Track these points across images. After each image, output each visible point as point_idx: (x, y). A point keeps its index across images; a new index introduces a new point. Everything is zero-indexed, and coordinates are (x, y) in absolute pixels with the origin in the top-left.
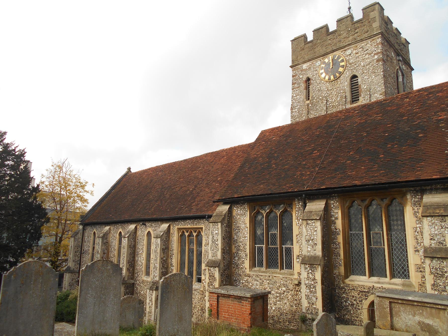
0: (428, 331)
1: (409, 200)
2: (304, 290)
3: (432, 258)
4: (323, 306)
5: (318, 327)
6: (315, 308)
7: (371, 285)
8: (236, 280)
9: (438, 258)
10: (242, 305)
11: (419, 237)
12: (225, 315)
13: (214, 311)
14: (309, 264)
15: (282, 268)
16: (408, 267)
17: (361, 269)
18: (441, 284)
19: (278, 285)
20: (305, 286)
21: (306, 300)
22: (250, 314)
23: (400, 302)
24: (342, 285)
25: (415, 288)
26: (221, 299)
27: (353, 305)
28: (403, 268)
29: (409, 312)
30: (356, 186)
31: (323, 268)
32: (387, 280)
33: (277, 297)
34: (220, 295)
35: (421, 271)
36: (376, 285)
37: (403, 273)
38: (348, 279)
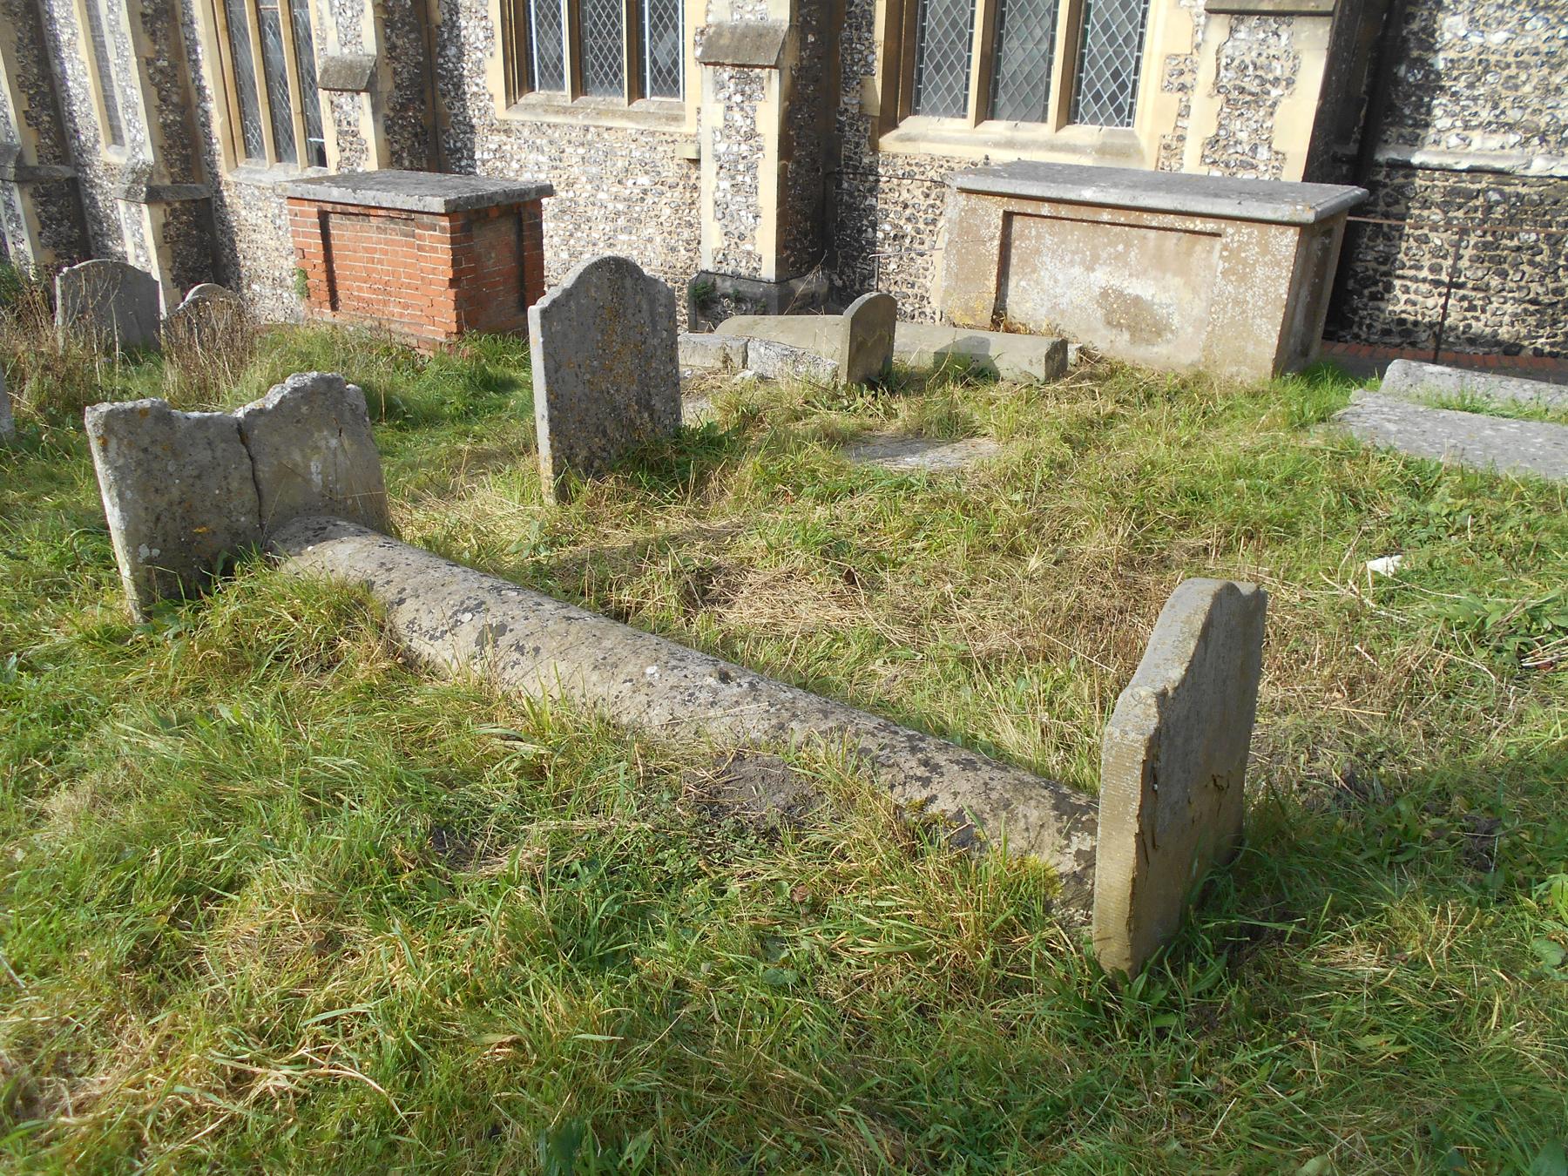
0: (1129, 327)
2: (710, 180)
3: (1241, 14)
4: (781, 246)
5: (556, 327)
6: (749, 253)
7: (977, 154)
8: (458, 150)
10: (420, 248)
12: (360, 289)
13: (318, 278)
14: (734, 65)
15: (637, 92)
16: (1137, 71)
17: (950, 89)
18: (1243, 136)
19: (620, 164)
20: (715, 167)
21: (717, 225)
22: (453, 283)
23: (1046, 209)
24: (866, 160)
25: (1142, 159)
26: (340, 227)
28: (1116, 75)
29: (1074, 253)
31: (794, 81)
32: (1046, 131)
33: (618, 214)
34: (329, 208)
35: (1182, 88)
37: (1113, 98)
38: (894, 133)
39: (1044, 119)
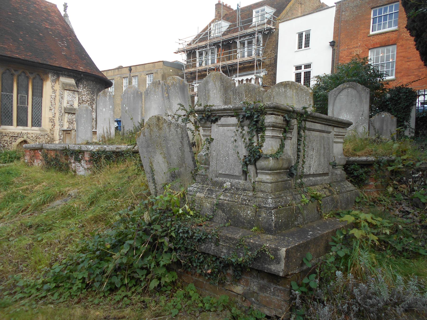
1: (50, 78)
3: (69, 113)
7: (20, 132)
9: (72, 113)
11: (53, 101)
27: (4, 146)
30: (20, 59)
36: (23, 132)
37: (38, 123)
39: (27, 126)
